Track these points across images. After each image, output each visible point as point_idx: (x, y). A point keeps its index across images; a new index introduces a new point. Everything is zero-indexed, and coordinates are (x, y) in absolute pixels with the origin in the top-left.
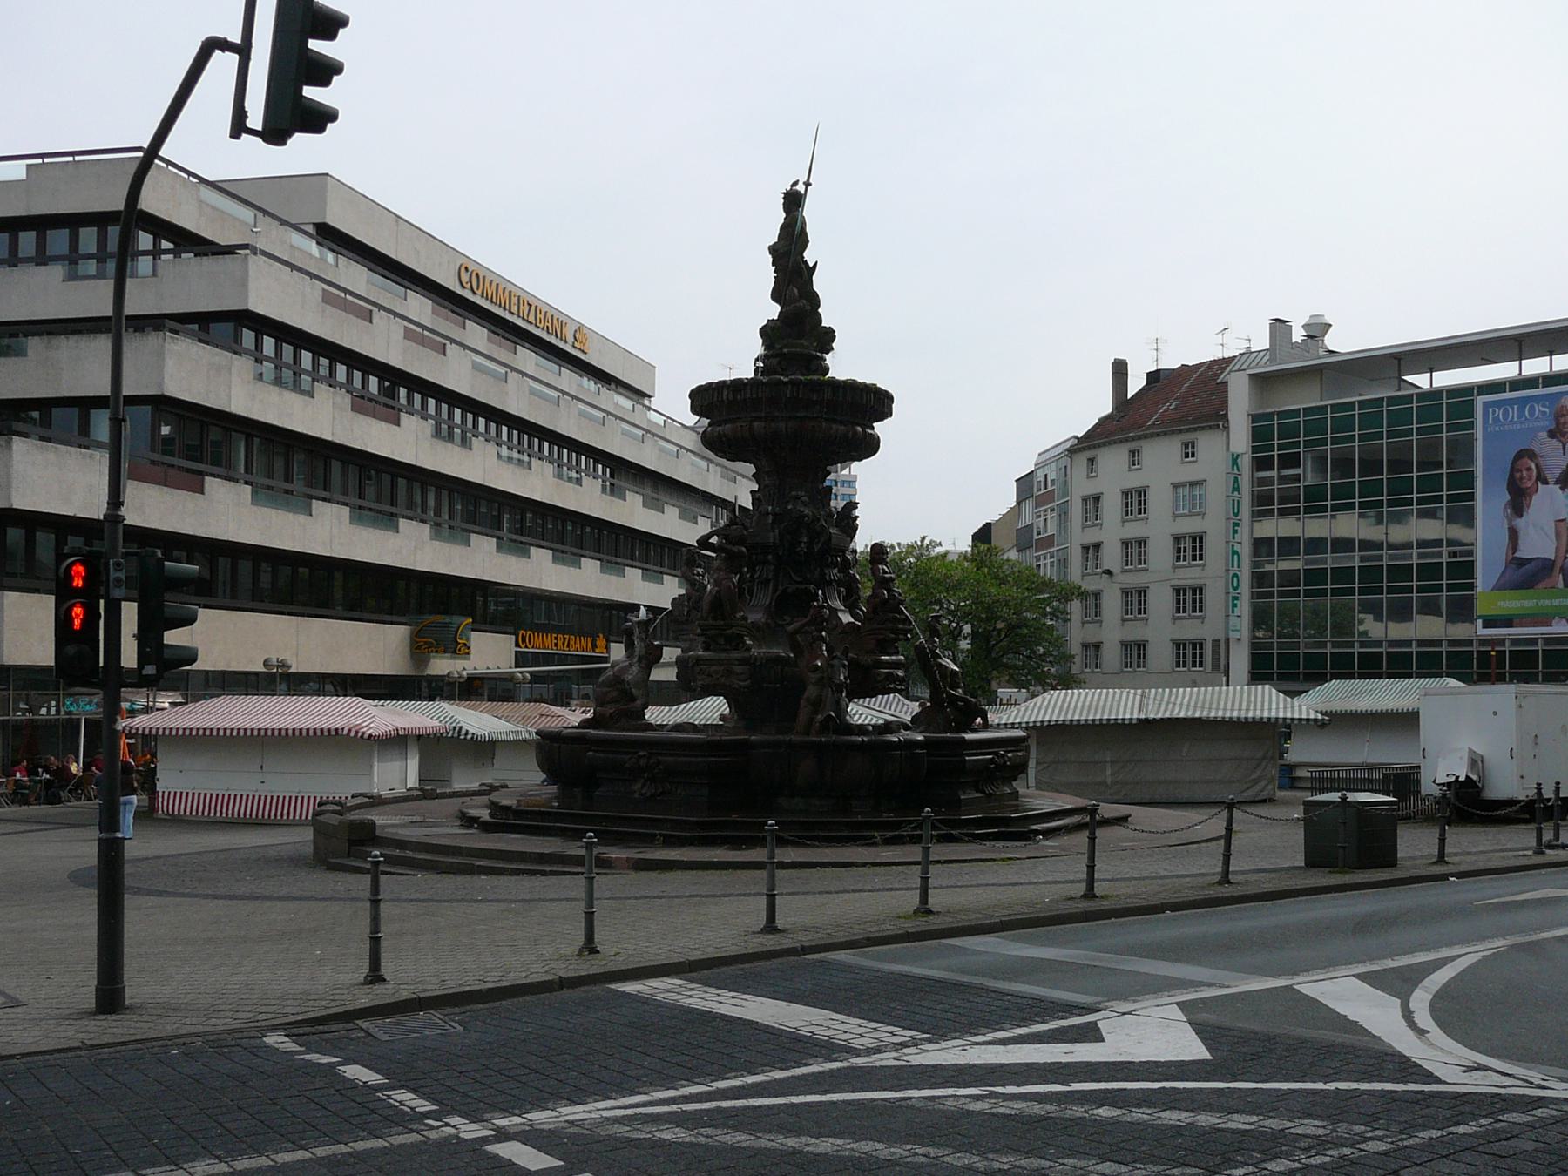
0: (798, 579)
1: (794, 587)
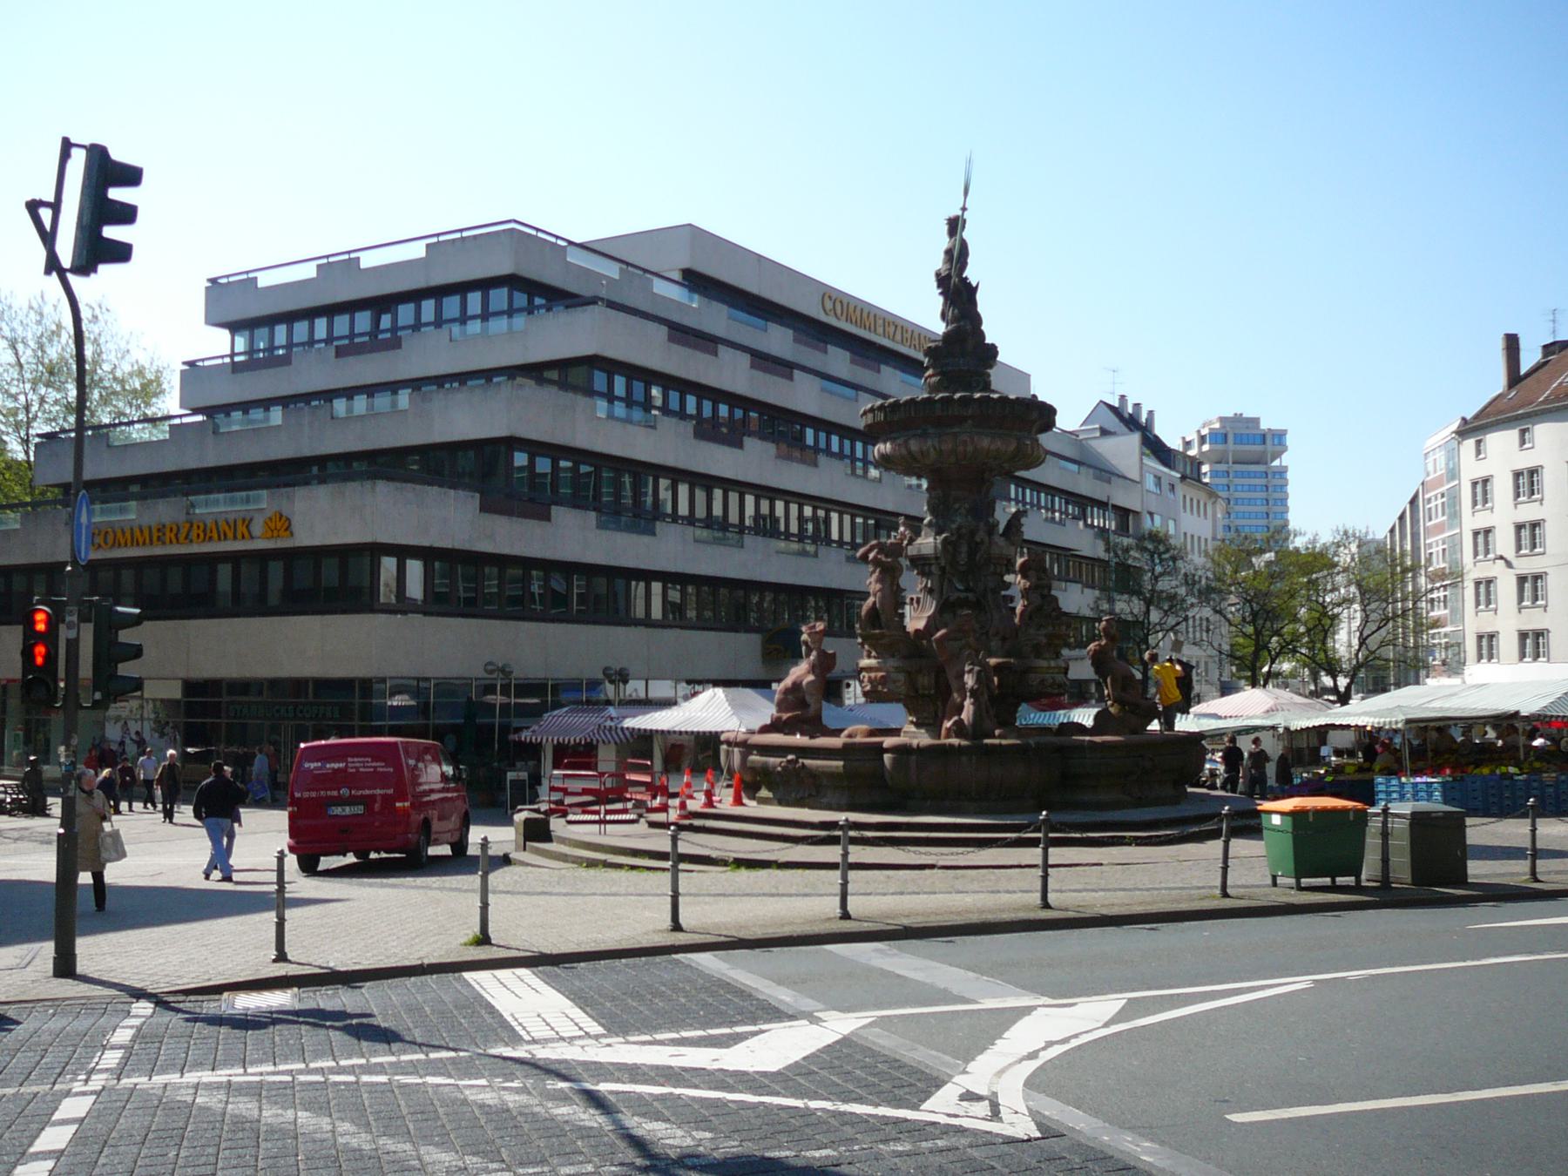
0: (961, 587)
1: (957, 595)
